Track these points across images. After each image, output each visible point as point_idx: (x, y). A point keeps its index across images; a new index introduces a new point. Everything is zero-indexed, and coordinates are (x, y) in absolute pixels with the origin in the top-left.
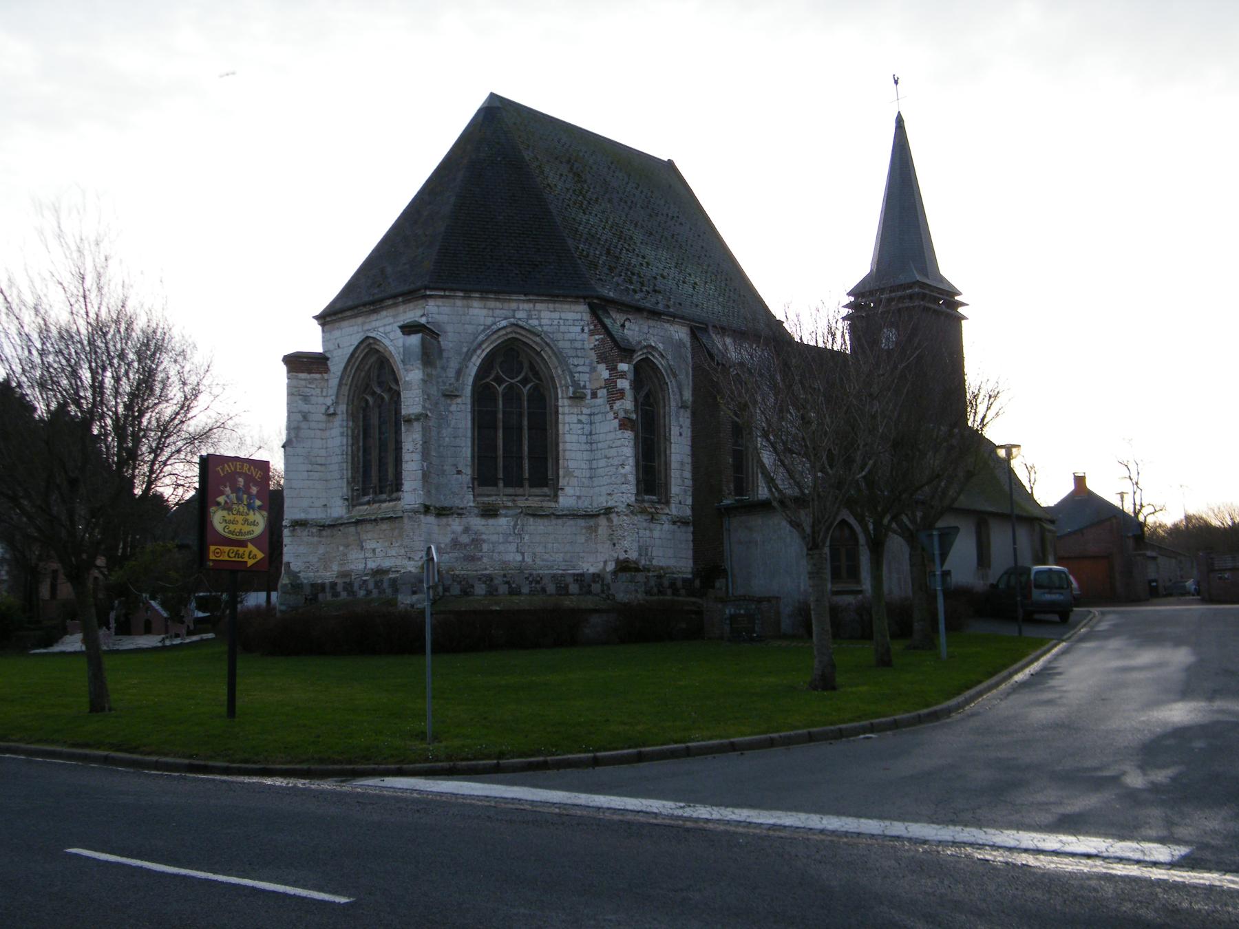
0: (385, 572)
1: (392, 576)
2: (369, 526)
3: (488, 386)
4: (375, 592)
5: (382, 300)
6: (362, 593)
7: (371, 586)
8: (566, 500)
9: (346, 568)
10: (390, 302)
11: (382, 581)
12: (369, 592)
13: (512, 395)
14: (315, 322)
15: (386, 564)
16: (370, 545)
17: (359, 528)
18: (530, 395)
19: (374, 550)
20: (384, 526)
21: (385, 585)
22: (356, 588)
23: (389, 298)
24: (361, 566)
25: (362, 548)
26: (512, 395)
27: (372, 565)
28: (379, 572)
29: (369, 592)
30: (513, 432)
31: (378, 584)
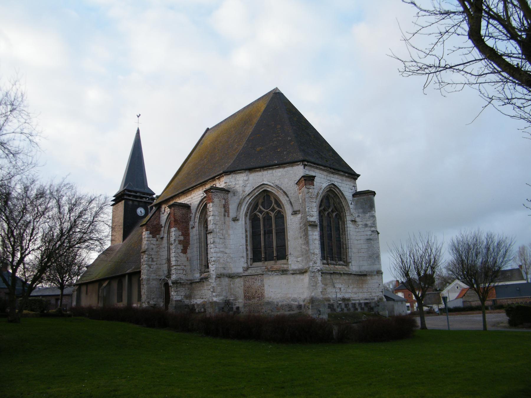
0: (349, 300)
1: (353, 302)
2: (337, 276)
3: (255, 214)
4: (345, 309)
5: (339, 171)
6: (339, 310)
7: (343, 306)
8: (354, 267)
9: (326, 296)
10: (342, 173)
11: (348, 304)
12: (342, 310)
13: (267, 218)
14: (358, 173)
15: (347, 296)
16: (338, 286)
17: (332, 276)
18: (264, 218)
19: (340, 289)
20: (345, 277)
21: (350, 306)
22: (335, 307)
23: (343, 171)
24: (334, 296)
25: (334, 287)
26: (267, 218)
27: (339, 296)
28: (344, 300)
29: (342, 310)
30: (268, 233)
31: (346, 305)
